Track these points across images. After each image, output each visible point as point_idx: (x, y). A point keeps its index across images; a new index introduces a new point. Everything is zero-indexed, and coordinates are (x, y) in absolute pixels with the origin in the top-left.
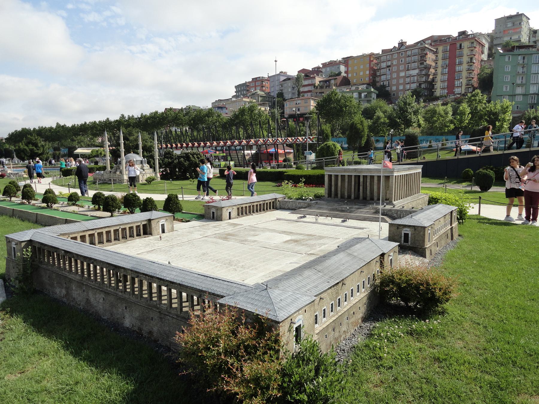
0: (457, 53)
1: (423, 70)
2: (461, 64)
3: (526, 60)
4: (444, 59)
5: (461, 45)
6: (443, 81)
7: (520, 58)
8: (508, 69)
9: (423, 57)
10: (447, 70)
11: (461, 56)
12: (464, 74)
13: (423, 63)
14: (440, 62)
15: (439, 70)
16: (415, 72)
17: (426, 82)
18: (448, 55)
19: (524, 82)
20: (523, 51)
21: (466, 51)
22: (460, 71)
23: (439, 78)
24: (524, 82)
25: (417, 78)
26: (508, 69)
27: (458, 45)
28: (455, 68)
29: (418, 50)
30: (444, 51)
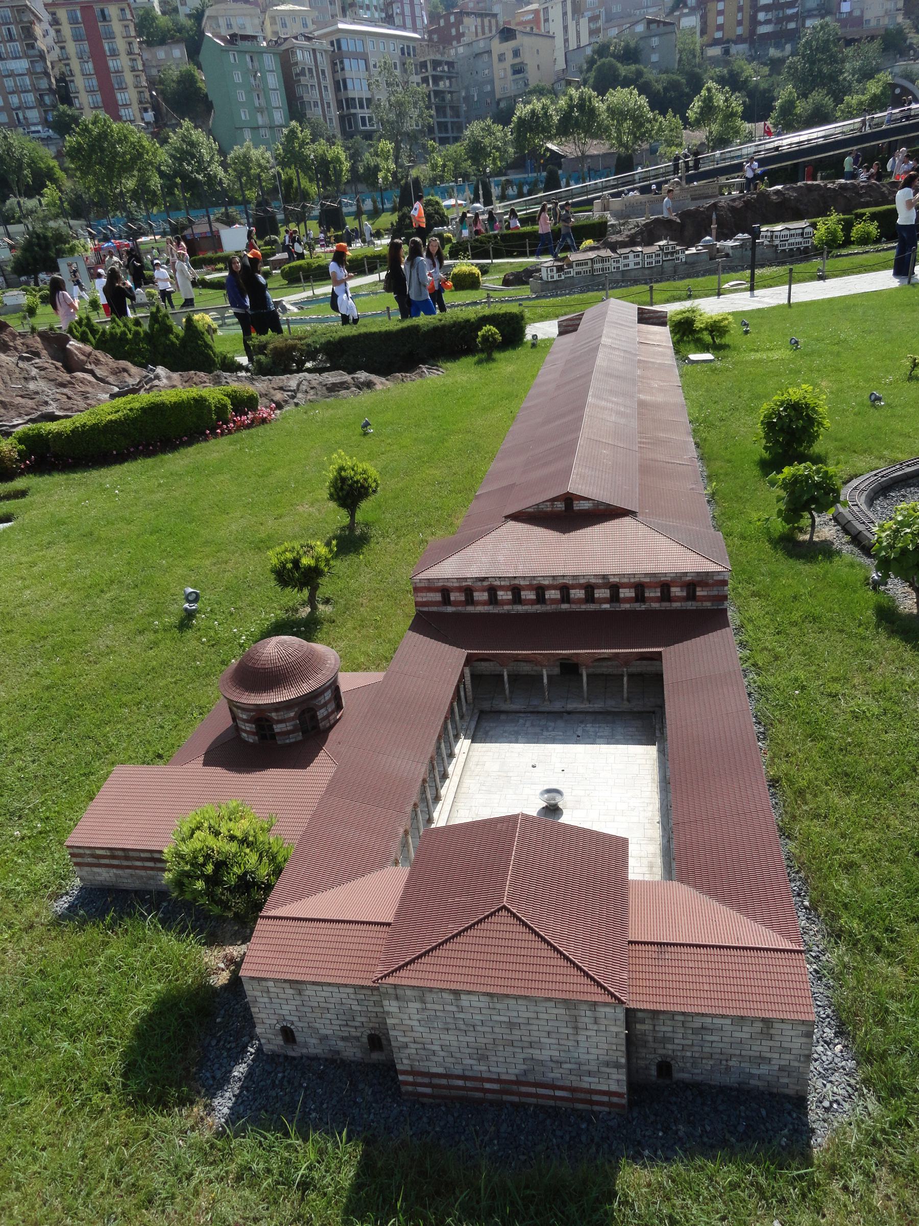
0: (101, 29)
1: (37, 61)
2: (114, 53)
3: (256, 64)
4: (77, 39)
5: (102, 11)
6: (90, 92)
7: (248, 59)
8: (238, 78)
9: (28, 33)
10: (91, 65)
11: (111, 36)
12: (129, 78)
13: (32, 46)
14: (72, 48)
15: (75, 65)
16: (22, 65)
17: (50, 89)
18: (83, 31)
19: (263, 102)
20: (247, 44)
21: (117, 27)
22: (118, 72)
23: (79, 83)
24: (263, 101)
25: (31, 80)
26: (238, 78)
27: (98, 13)
28: (106, 63)
29: (12, 12)
30: (73, 21)
